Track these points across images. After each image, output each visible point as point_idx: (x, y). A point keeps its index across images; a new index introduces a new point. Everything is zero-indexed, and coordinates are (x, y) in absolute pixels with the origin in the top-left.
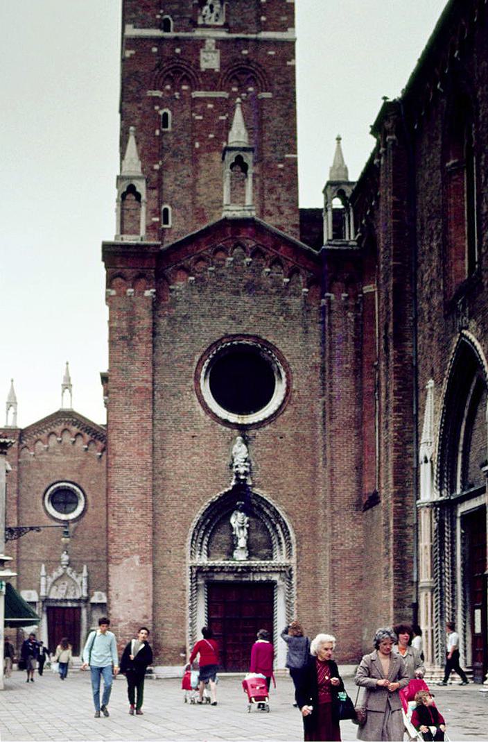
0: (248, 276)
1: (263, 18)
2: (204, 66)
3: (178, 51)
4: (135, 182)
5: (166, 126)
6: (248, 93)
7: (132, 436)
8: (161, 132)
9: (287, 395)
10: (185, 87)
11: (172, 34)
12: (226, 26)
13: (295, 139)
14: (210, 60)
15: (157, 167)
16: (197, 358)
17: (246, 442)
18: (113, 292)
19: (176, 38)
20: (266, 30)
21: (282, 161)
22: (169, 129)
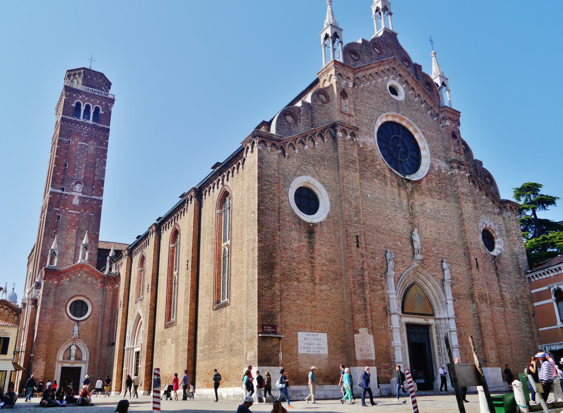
0: (84, 279)
1: (93, 192)
2: (74, 203)
3: (66, 197)
4: (55, 251)
5: (59, 219)
6: (86, 213)
7: (45, 322)
8: (57, 221)
9: (91, 313)
10: (67, 208)
11: (64, 192)
12: (82, 193)
13: (99, 228)
14: (76, 201)
15: (54, 231)
16: (67, 301)
17: (78, 326)
18: (45, 281)
19: (66, 194)
20: (94, 196)
21: (94, 234)
22: (60, 220)
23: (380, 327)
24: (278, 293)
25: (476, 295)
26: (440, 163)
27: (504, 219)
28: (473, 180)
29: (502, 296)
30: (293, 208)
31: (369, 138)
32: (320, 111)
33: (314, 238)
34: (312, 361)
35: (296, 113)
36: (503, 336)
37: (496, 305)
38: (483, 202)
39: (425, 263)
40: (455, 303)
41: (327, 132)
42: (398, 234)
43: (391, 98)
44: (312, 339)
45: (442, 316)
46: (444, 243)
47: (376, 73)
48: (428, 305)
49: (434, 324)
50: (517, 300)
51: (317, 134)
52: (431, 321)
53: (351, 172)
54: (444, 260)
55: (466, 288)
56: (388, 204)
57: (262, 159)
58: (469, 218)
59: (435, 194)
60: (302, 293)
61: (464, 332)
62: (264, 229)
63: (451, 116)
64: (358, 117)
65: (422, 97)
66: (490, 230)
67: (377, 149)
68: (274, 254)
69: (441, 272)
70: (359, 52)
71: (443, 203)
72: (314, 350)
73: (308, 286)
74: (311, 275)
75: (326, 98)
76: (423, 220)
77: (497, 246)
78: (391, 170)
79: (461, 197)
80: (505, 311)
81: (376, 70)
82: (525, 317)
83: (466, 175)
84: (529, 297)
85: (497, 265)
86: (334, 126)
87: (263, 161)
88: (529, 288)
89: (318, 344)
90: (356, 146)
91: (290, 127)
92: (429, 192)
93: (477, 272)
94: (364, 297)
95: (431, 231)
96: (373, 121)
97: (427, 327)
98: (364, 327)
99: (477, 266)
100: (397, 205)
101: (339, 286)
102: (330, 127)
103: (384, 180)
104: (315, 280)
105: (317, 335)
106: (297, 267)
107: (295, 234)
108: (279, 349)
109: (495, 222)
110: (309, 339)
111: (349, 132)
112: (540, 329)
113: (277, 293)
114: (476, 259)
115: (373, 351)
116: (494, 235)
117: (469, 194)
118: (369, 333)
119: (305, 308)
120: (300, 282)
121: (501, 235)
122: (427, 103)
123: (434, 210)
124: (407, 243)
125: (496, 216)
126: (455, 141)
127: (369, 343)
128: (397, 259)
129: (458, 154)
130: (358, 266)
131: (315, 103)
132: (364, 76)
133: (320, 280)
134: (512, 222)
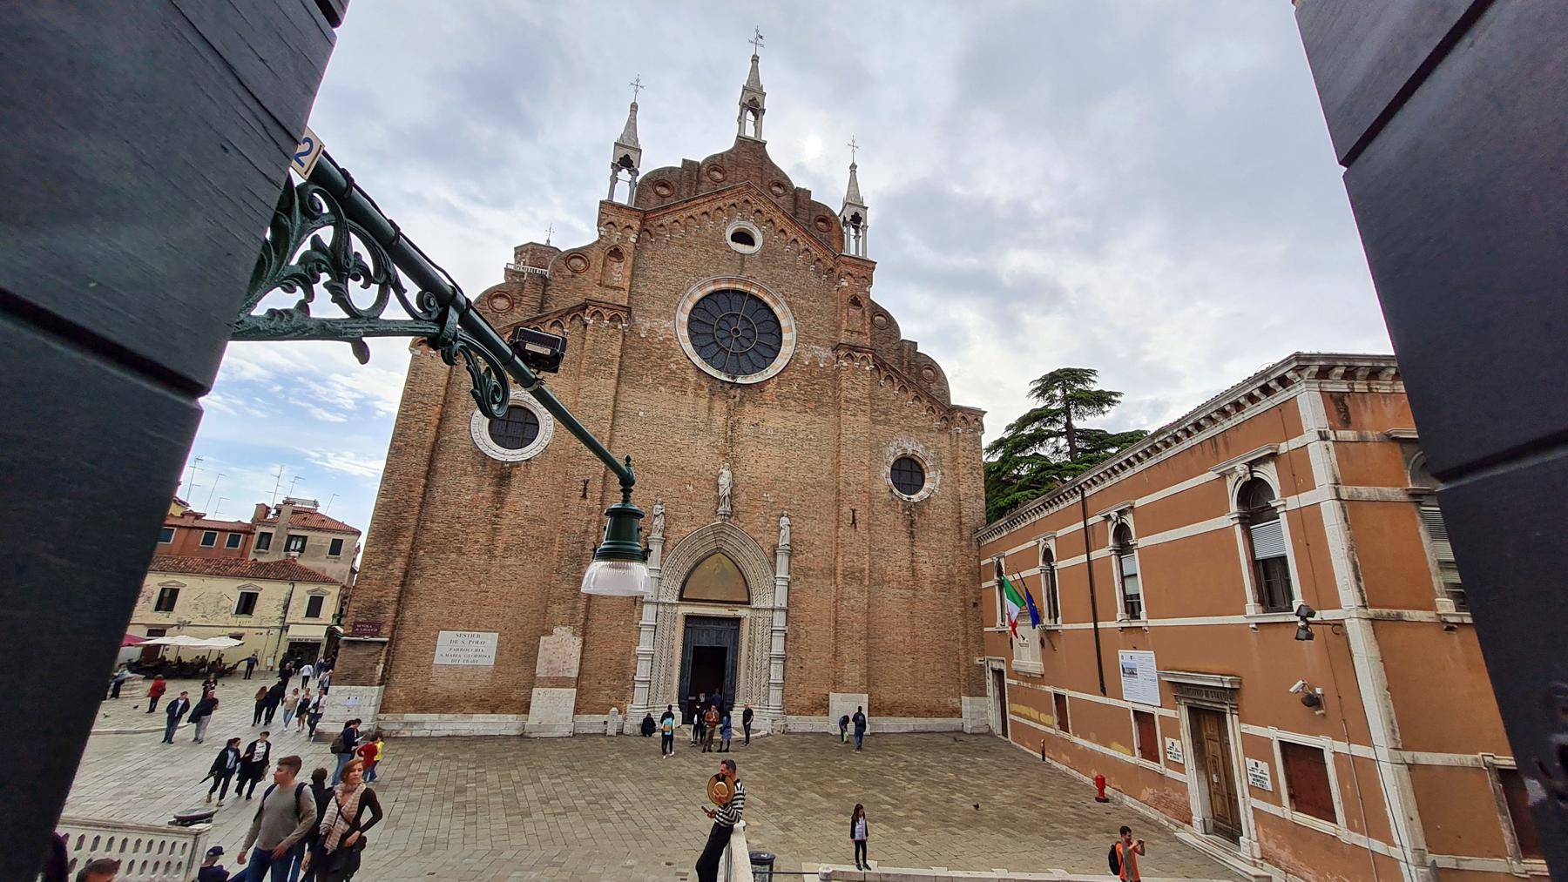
23: (615, 623)
24: (398, 573)
25: (839, 571)
26: (818, 350)
27: (951, 438)
28: (889, 376)
29: (914, 572)
30: (476, 441)
31: (664, 321)
32: (564, 286)
33: (509, 484)
34: (458, 675)
35: (515, 293)
36: (901, 638)
37: (895, 586)
38: (906, 411)
39: (741, 519)
40: (797, 583)
41: (571, 320)
42: (692, 473)
43: (729, 250)
44: (467, 642)
45: (763, 606)
46: (793, 484)
47: (706, 213)
48: (742, 586)
49: (748, 617)
50: (950, 575)
51: (550, 323)
52: (742, 612)
53: (597, 380)
54: (785, 512)
55: (829, 559)
56: (680, 425)
57: (418, 369)
58: (854, 441)
59: (793, 403)
60: (463, 572)
61: (807, 632)
62: (396, 476)
63: (850, 269)
64: (649, 289)
65: (801, 243)
66: (916, 459)
67: (677, 338)
68: (406, 515)
69: (775, 533)
70: (674, 184)
71: (808, 417)
72: (466, 659)
73: (481, 561)
74: (486, 544)
75: (585, 263)
76: (754, 449)
77: (926, 485)
78: (699, 370)
79: (843, 407)
80: (914, 595)
81: (705, 208)
82: (961, 607)
83: (867, 368)
84: (972, 573)
85: (916, 518)
86: (584, 307)
87: (419, 372)
88: (976, 556)
89: (476, 650)
90: (620, 336)
91: (497, 317)
92: (781, 401)
93: (852, 532)
94: (579, 578)
95: (768, 466)
96: (679, 292)
97: (737, 621)
98: (565, 626)
99: (854, 522)
100: (701, 426)
101: (542, 559)
102: (581, 310)
103: (682, 387)
104: (495, 550)
105: (478, 636)
106: (463, 532)
107: (470, 481)
108: (379, 659)
109: (929, 444)
110: (460, 642)
111: (607, 314)
112: (986, 629)
113: (397, 572)
114: (854, 511)
115: (575, 664)
116: (924, 467)
117: (867, 401)
118: (574, 634)
119: (463, 593)
120: (464, 554)
121: (935, 468)
122: (810, 252)
123: (784, 430)
124: (708, 487)
125: (934, 434)
126: (859, 312)
127: (569, 650)
128: (679, 513)
129: (855, 335)
130: (576, 529)
131: (557, 274)
132: (677, 221)
133: (505, 550)
134: (961, 444)
